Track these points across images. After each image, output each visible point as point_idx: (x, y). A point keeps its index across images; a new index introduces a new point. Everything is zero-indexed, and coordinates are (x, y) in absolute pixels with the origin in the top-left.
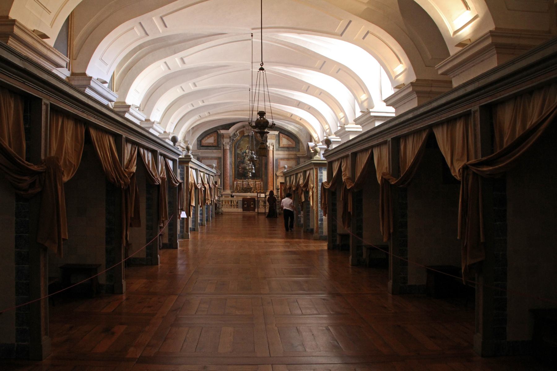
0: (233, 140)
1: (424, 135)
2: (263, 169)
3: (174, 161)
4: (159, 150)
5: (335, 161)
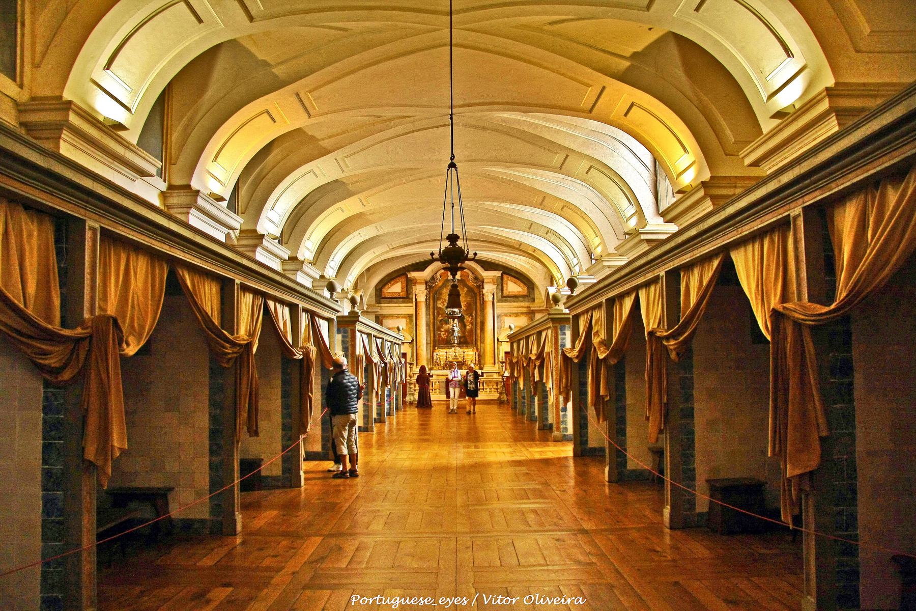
0: (431, 287)
1: (716, 263)
2: (479, 332)
3: (329, 320)
4: (302, 304)
5: (582, 313)
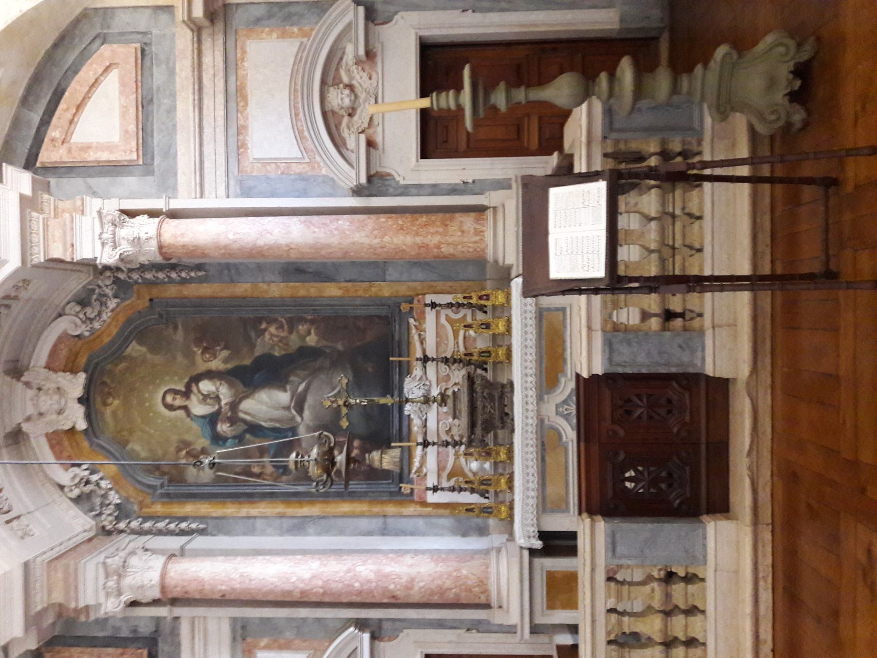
2: (332, 290)
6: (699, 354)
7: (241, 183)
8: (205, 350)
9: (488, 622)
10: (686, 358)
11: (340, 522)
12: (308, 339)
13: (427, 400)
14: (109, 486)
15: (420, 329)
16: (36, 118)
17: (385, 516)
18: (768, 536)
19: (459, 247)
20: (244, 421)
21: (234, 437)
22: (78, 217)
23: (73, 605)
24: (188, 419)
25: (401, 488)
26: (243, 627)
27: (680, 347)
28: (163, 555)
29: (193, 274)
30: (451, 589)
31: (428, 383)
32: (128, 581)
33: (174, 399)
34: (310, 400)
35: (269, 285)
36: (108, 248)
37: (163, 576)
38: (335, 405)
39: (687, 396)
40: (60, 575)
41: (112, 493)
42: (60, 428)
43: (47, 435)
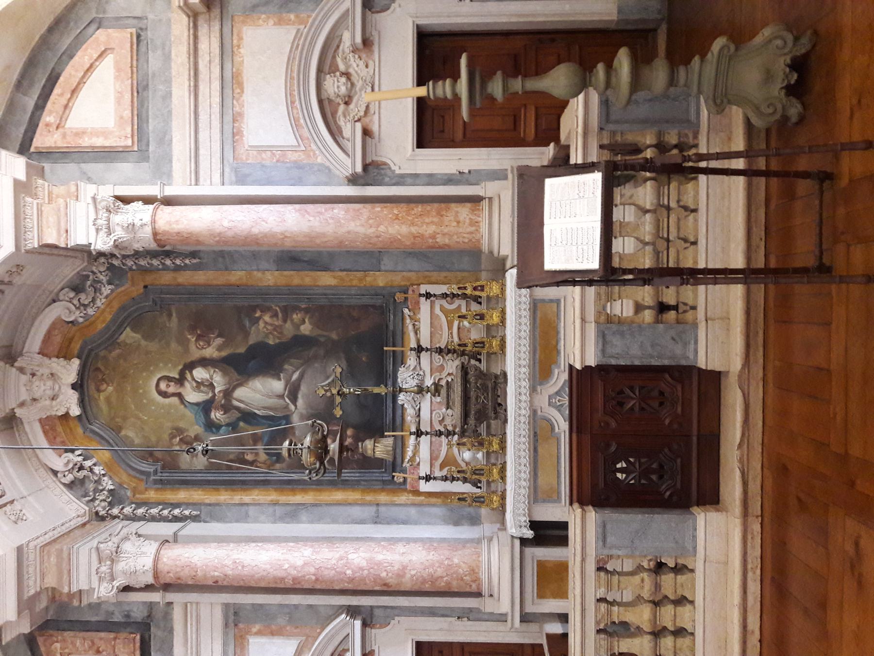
0: (115, 498)
2: (326, 279)
6: (692, 346)
7: (236, 171)
8: (199, 338)
9: (478, 610)
10: (678, 350)
11: (334, 510)
12: (302, 327)
13: (421, 390)
14: (103, 472)
15: (415, 320)
16: (30, 103)
17: (378, 505)
18: (756, 527)
19: (455, 237)
20: (238, 409)
21: (228, 425)
22: (72, 203)
23: (66, 590)
24: (182, 406)
25: (394, 477)
26: (235, 613)
27: (673, 339)
28: (156, 541)
29: (187, 261)
30: (442, 577)
31: (421, 373)
32: (121, 566)
33: (168, 386)
34: (303, 389)
35: (263, 274)
36: (102, 234)
37: (156, 561)
38: (328, 394)
39: (679, 389)
40: (53, 559)
41: (106, 478)
42: (54, 413)
43: (40, 420)
